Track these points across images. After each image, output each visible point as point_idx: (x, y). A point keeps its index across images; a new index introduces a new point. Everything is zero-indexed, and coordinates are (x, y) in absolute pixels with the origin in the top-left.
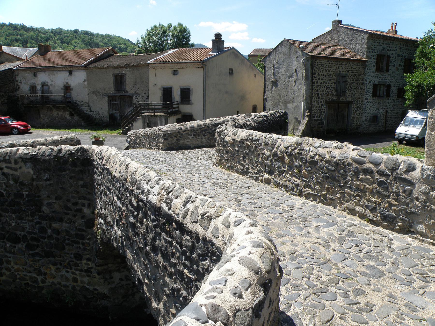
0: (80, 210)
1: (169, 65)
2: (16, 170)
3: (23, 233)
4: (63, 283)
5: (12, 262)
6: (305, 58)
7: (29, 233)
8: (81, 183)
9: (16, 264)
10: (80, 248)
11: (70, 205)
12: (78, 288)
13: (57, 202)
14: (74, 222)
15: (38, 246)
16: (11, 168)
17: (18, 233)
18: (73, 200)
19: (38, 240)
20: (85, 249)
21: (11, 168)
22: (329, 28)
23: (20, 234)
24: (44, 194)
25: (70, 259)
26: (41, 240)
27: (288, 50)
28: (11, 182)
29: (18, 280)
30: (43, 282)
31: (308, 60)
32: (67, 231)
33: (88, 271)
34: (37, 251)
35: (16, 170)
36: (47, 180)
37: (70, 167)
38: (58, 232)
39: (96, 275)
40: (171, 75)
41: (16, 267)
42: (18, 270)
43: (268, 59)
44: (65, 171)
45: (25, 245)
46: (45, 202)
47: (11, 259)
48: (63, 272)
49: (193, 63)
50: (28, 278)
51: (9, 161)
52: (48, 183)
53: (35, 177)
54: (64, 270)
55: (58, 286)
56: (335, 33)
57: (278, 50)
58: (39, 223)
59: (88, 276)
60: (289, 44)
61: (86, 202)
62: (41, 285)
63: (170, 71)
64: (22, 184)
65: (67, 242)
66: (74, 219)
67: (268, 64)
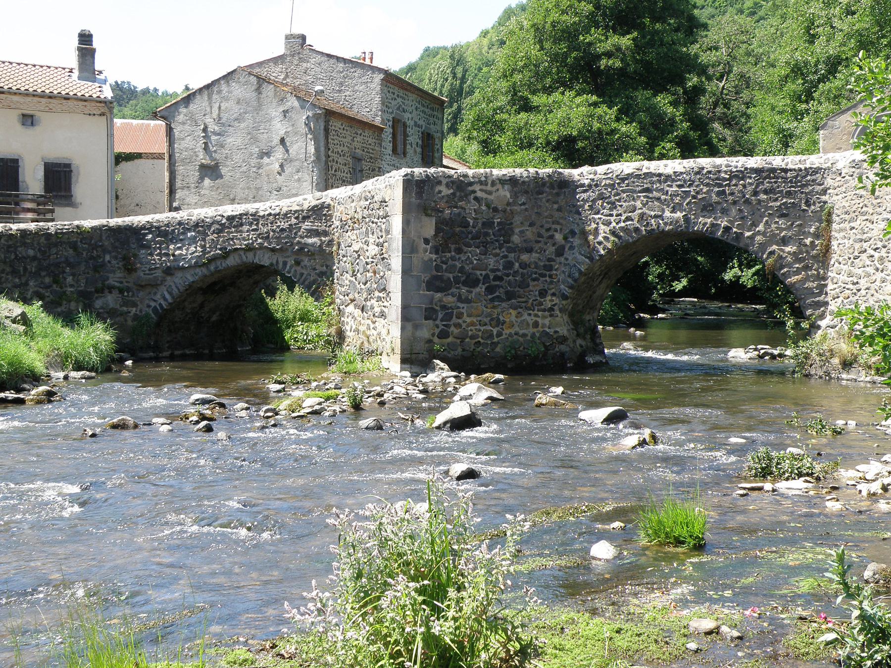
0: (552, 237)
1: (15, 98)
2: (490, 193)
3: (484, 273)
4: (521, 332)
5: (465, 314)
6: (310, 114)
7: (493, 271)
8: (556, 206)
9: (469, 316)
10: (546, 281)
11: (543, 231)
12: (538, 335)
13: (530, 228)
14: (545, 251)
15: (499, 287)
16: (486, 192)
17: (478, 273)
18: (547, 226)
19: (500, 279)
20: (551, 283)
21: (486, 192)
22: (279, 49)
23: (481, 275)
24: (517, 220)
25: (534, 298)
26: (505, 278)
27: (254, 94)
28: (484, 208)
29: (467, 340)
30: (499, 334)
31: (317, 120)
32: (536, 263)
33: (551, 309)
34: (497, 294)
35: (490, 193)
36: (524, 204)
37: (547, 190)
38: (523, 265)
39: (558, 312)
40: (19, 127)
41: (468, 320)
42: (472, 324)
43: (183, 110)
44: (542, 194)
45: (484, 287)
46: (517, 231)
47: (464, 311)
48: (525, 316)
49: (85, 101)
50: (480, 334)
51: (485, 183)
52: (523, 207)
53: (511, 200)
54: (526, 314)
55: (515, 337)
56: (296, 62)
57: (219, 92)
58: (505, 257)
59: (551, 316)
60: (253, 79)
61: (558, 227)
62: (496, 340)
63: (13, 116)
64: (495, 210)
65: (534, 276)
66: (545, 247)
67: (184, 123)
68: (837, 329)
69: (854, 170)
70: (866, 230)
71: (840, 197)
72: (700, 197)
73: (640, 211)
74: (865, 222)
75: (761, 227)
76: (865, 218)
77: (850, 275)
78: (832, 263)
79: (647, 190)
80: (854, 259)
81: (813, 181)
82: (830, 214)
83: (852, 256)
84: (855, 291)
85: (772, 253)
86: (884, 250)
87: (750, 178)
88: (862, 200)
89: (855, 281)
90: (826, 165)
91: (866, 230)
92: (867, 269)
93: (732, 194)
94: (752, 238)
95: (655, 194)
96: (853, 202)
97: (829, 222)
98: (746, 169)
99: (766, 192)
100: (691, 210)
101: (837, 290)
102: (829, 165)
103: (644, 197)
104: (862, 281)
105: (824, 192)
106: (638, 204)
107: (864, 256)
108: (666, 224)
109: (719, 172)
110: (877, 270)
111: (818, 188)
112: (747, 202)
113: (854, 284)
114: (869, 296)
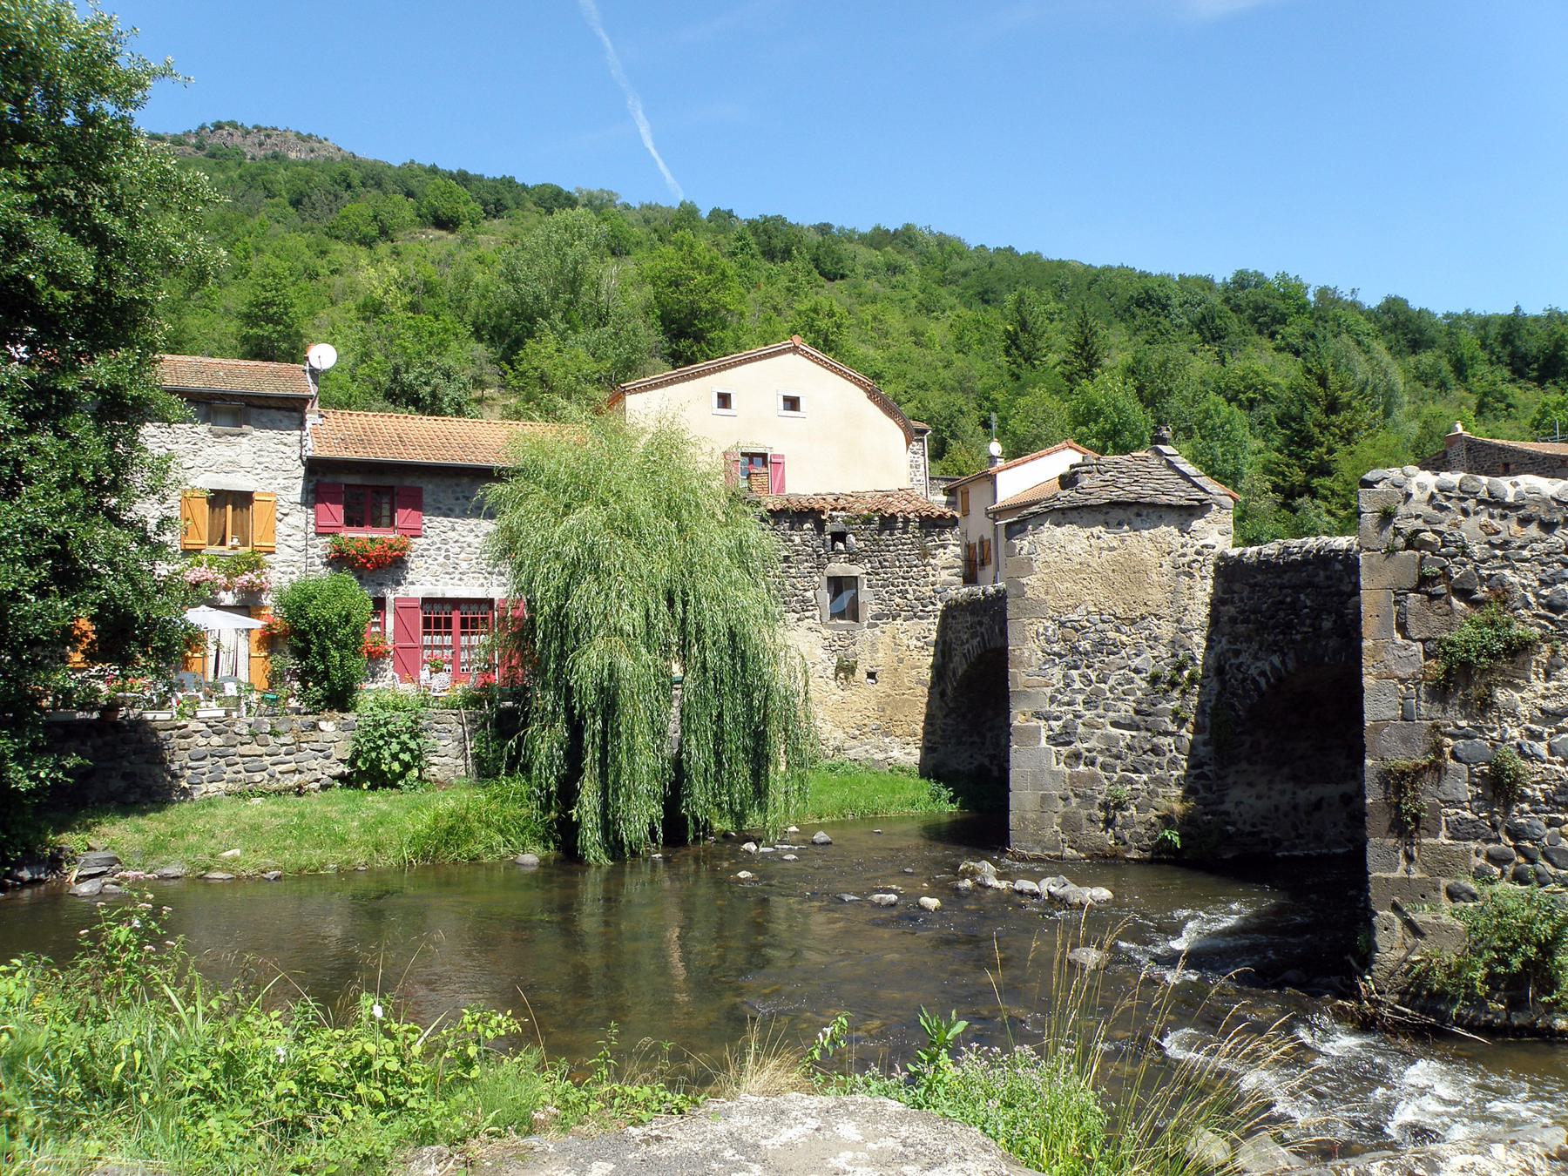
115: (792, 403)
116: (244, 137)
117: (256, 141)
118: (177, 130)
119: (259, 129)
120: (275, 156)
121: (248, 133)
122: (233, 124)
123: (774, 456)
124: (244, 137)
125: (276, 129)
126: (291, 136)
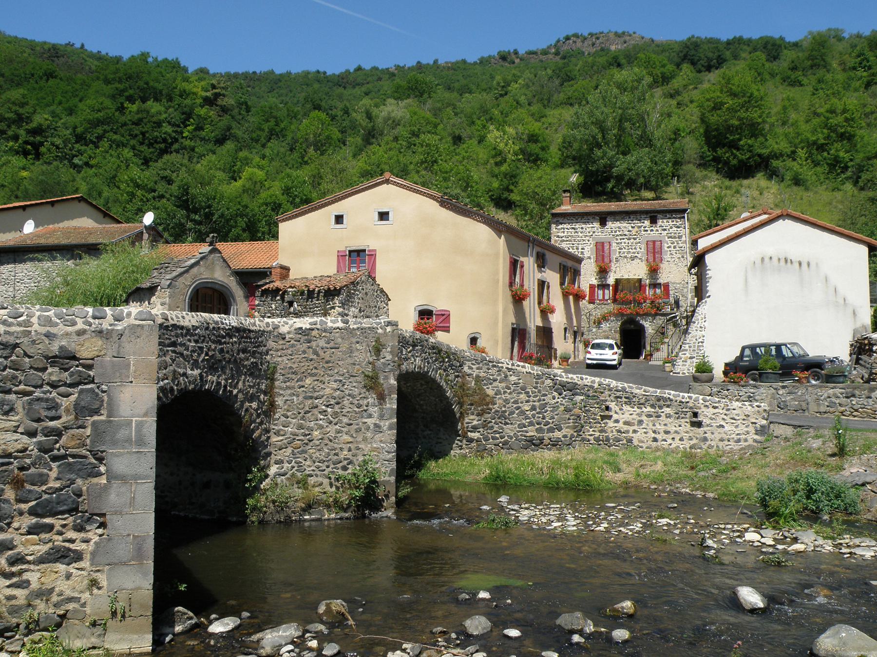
68: (288, 476)
69: (300, 336)
70: (318, 389)
71: (285, 358)
72: (210, 353)
73: (171, 368)
74: (316, 382)
75: (240, 385)
76: (315, 378)
77: (300, 427)
78: (277, 416)
79: (174, 344)
80: (305, 413)
81: (262, 342)
82: (273, 373)
83: (302, 412)
84: (306, 441)
85: (247, 410)
86: (337, 407)
87: (235, 336)
88: (312, 362)
89: (307, 432)
90: (269, 329)
91: (318, 389)
92: (321, 422)
93: (228, 352)
94: (236, 396)
95: (179, 349)
96: (303, 364)
97: (273, 380)
98: (233, 327)
99: (244, 351)
100: (204, 367)
101: (285, 441)
102: (270, 328)
103: (171, 351)
104: (316, 433)
105: (267, 353)
106: (168, 359)
107: (315, 411)
108: (190, 382)
109: (219, 328)
110: (331, 423)
111: (265, 349)
112: (235, 360)
113: (306, 435)
114: (322, 445)
115: (383, 216)
116: (583, 42)
117: (590, 43)
118: (544, 46)
119: (591, 35)
120: (602, 50)
121: (585, 39)
122: (576, 36)
123: (369, 251)
124: (583, 42)
125: (602, 33)
126: (612, 35)
